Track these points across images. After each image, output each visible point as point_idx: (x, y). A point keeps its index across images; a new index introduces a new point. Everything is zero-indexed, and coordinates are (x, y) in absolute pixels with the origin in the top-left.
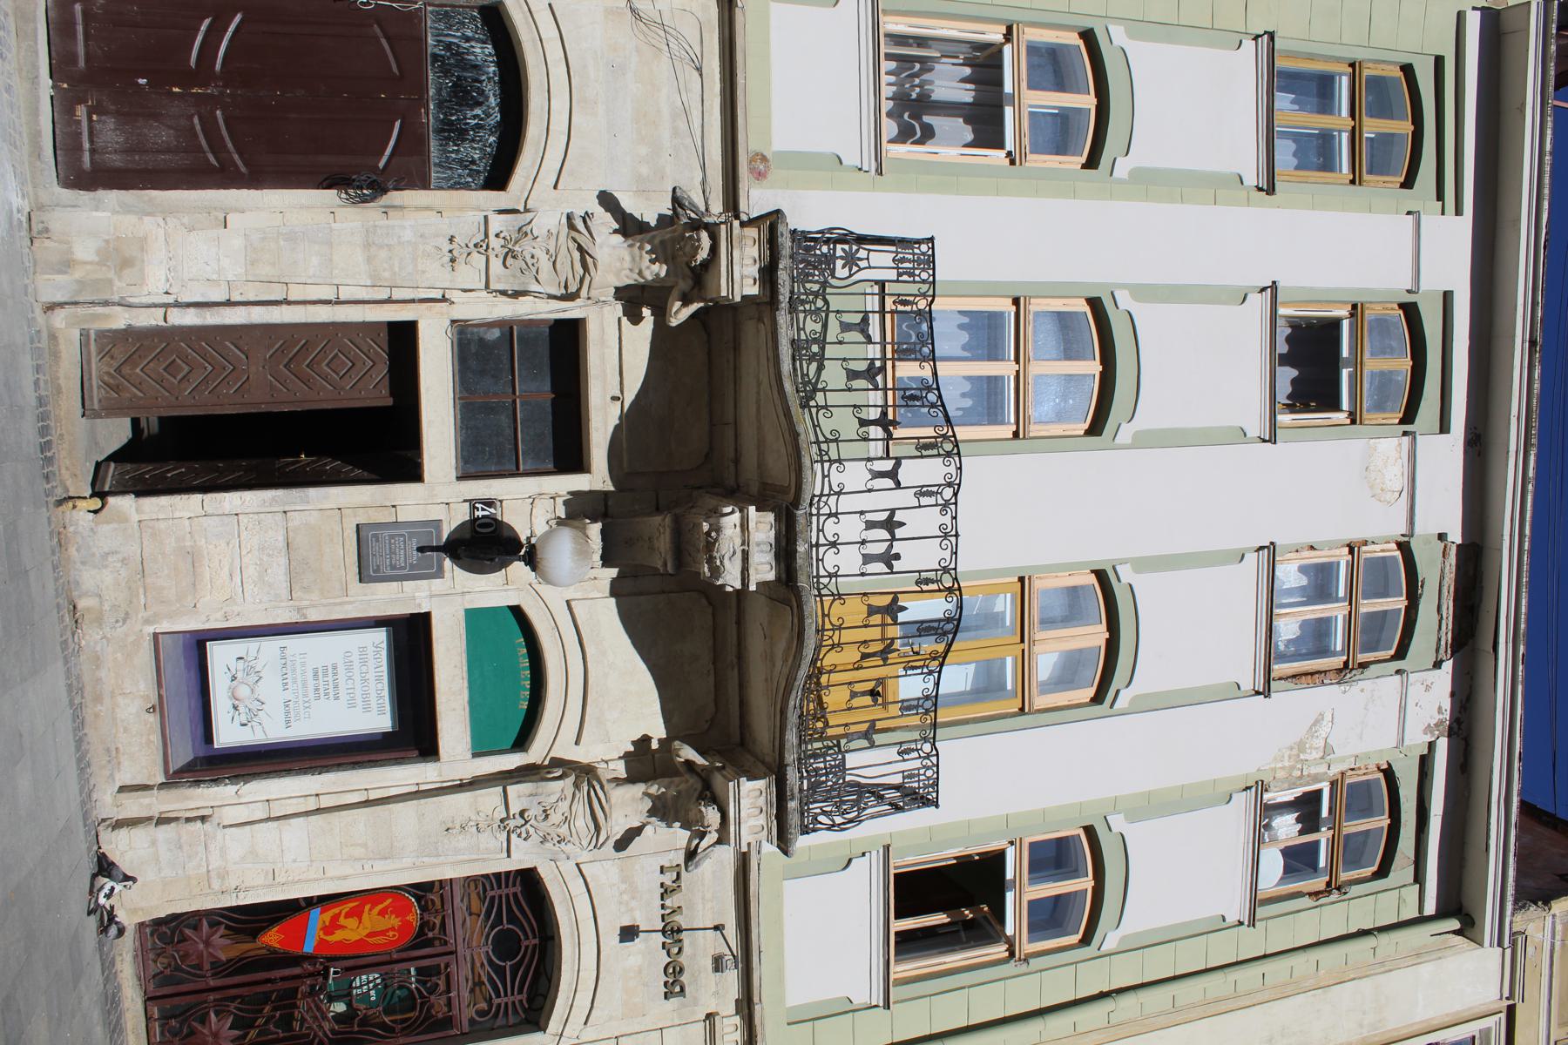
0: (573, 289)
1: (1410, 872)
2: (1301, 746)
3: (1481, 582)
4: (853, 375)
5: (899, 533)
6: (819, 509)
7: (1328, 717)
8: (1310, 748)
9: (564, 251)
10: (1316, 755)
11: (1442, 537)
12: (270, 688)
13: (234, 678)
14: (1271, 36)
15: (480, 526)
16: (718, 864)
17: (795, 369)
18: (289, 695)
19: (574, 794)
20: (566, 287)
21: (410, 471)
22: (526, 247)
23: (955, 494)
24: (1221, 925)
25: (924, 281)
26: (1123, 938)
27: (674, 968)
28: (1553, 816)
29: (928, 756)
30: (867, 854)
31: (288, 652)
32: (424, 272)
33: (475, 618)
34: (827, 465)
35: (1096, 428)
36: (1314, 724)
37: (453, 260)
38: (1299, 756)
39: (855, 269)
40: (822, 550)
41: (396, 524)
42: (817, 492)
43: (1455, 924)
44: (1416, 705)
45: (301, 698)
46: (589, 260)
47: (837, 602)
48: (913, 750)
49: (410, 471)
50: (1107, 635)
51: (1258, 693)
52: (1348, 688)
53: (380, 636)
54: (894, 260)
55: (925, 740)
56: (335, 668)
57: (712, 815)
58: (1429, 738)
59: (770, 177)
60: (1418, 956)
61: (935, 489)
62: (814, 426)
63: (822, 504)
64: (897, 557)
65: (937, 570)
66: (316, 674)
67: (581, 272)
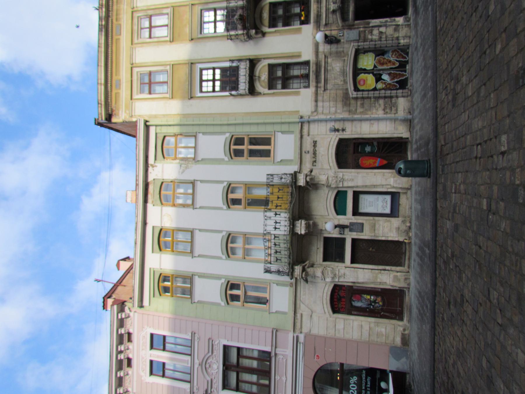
1: (158, 135)
2: (187, 168)
3: (144, 195)
5: (274, 227)
7: (180, 173)
9: (326, 275)
10: (183, 166)
11: (154, 205)
12: (380, 204)
13: (386, 207)
14: (192, 303)
16: (306, 169)
21: (354, 241)
22: (332, 276)
24: (204, 133)
33: (344, 213)
37: (344, 274)
41: (357, 232)
43: (148, 124)
49: (354, 241)
57: (308, 179)
58: (156, 164)
60: (156, 116)
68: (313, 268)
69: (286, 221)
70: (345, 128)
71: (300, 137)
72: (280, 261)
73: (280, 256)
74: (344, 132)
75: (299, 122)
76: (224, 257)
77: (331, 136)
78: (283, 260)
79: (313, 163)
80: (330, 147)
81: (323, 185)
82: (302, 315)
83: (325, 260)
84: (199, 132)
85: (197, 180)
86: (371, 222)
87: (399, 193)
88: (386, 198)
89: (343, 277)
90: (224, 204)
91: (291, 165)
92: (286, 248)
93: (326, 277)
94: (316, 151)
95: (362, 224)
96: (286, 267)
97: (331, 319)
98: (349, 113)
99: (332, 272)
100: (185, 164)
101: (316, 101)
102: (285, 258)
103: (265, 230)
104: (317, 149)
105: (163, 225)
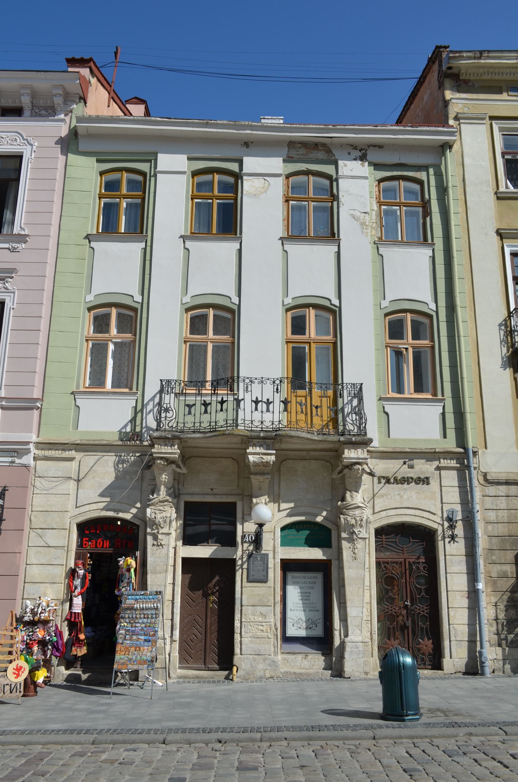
2: (363, 224)
5: (260, 399)
6: (249, 427)
7: (352, 212)
8: (364, 220)
13: (300, 628)
17: (203, 432)
25: (175, 384)
27: (418, 480)
28: (420, 78)
30: (384, 405)
31: (293, 608)
38: (367, 225)
39: (170, 409)
40: (263, 427)
42: (243, 428)
44: (352, 170)
48: (340, 392)
52: (341, 203)
53: (290, 575)
54: (168, 394)
58: (366, 164)
61: (245, 386)
62: (222, 427)
63: (248, 426)
64: (268, 400)
65: (274, 386)
69: (273, 424)
70: (457, 542)
71: (437, 450)
72: (187, 412)
73: (198, 415)
78: (190, 419)
79: (384, 477)
80: (418, 512)
83: (187, 504)
88: (316, 626)
91: (380, 433)
92: (216, 425)
98: (486, 549)
101: (507, 483)
103: (251, 381)
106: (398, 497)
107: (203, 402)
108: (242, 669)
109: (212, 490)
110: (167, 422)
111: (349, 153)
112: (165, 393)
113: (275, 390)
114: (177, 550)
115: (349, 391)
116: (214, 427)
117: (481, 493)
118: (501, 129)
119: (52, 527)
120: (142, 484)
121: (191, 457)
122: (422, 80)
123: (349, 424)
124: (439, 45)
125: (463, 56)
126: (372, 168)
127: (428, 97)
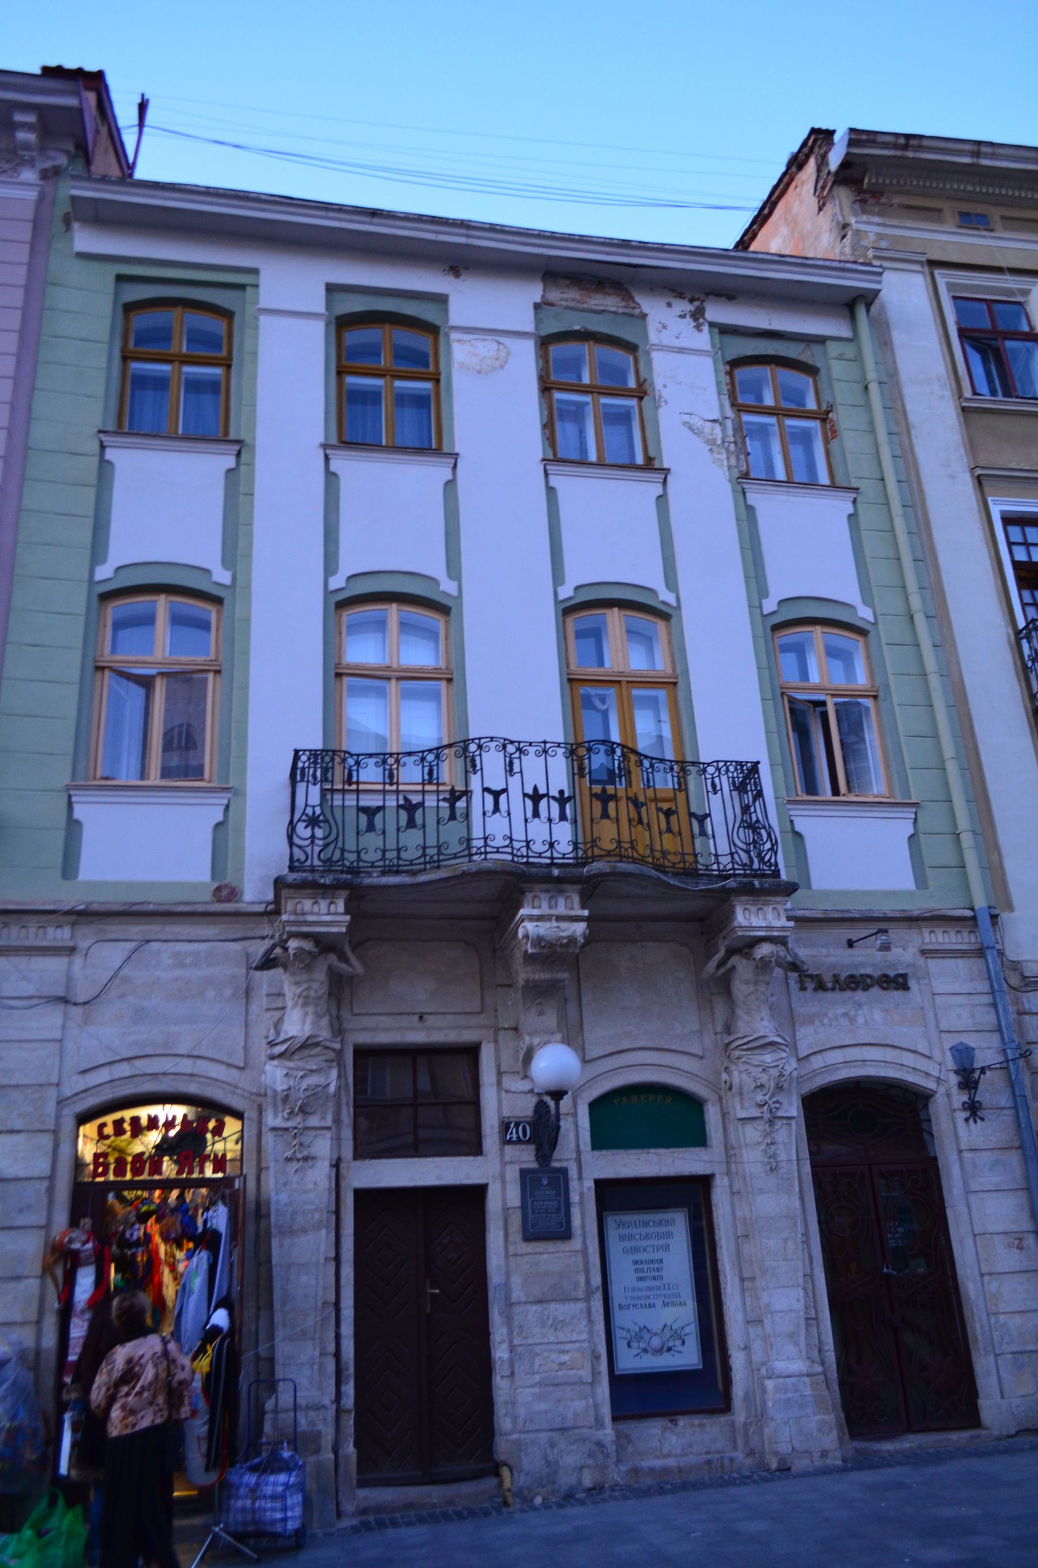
0: (331, 1055)
1: (816, 348)
2: (712, 442)
4: (411, 823)
5: (542, 790)
6: (523, 856)
7: (687, 418)
8: (712, 434)
9: (301, 1064)
10: (718, 430)
11: (537, 306)
13: (645, 1350)
14: (100, 432)
15: (525, 1135)
17: (407, 872)
18: (659, 1303)
19: (745, 1062)
20: (332, 1061)
23: (512, 742)
25: (332, 760)
26: (865, 602)
29: (718, 769)
31: (624, 1303)
32: (315, 1184)
33: (599, 1142)
34: (489, 849)
35: (442, 609)
36: (691, 428)
37: (306, 1159)
40: (555, 855)
41: (523, 1207)
42: (509, 857)
43: (861, 312)
45: (662, 1292)
46: (310, 1042)
47: (598, 843)
50: (616, 610)
51: (665, 479)
54: (315, 784)
55: (704, 771)
56: (636, 1262)
57: (764, 950)
58: (706, 328)
59: (234, 885)
60: (884, 343)
61: (508, 759)
64: (561, 792)
66: (641, 1279)
67: (318, 1049)
68: (326, 996)
70: (982, 1119)
71: (915, 913)
74: (967, 1114)
75: (972, 909)
76: (337, 582)
77: (937, 1054)
78: (372, 842)
80: (889, 1055)
81: (728, 1029)
82: (72, 950)
84: (858, 500)
85: (665, 482)
86: (582, 1279)
87: (726, 1407)
88: (683, 1343)
89: (288, 1154)
90: (577, 588)
92: (439, 853)
93: (291, 1064)
94: (866, 989)
95: (565, 1234)
96: (337, 856)
97: (51, 1107)
99: (316, 1094)
100: (723, 442)
102: (384, 851)
103: (519, 750)
104: (875, 991)
105: (454, 336)
106: (844, 1021)
107: (401, 802)
108: (522, 1470)
109: (421, 1018)
110: (317, 849)
111: (669, 305)
112: (308, 781)
113: (576, 771)
114: (343, 1171)
115: (733, 778)
116: (435, 858)
117: (1015, 1008)
118: (950, 287)
119: (9, 1127)
120: (247, 1010)
121: (367, 940)
122: (766, 211)
123: (740, 852)
124: (817, 126)
125: (874, 142)
126: (717, 338)
127: (784, 241)
